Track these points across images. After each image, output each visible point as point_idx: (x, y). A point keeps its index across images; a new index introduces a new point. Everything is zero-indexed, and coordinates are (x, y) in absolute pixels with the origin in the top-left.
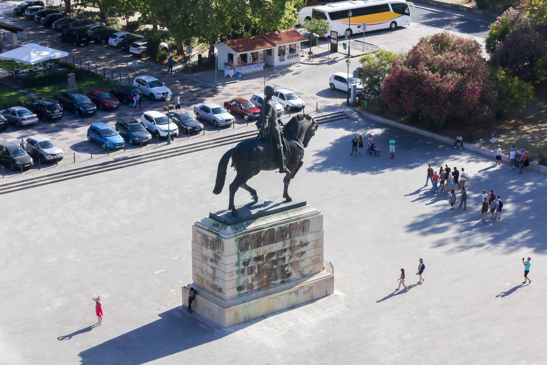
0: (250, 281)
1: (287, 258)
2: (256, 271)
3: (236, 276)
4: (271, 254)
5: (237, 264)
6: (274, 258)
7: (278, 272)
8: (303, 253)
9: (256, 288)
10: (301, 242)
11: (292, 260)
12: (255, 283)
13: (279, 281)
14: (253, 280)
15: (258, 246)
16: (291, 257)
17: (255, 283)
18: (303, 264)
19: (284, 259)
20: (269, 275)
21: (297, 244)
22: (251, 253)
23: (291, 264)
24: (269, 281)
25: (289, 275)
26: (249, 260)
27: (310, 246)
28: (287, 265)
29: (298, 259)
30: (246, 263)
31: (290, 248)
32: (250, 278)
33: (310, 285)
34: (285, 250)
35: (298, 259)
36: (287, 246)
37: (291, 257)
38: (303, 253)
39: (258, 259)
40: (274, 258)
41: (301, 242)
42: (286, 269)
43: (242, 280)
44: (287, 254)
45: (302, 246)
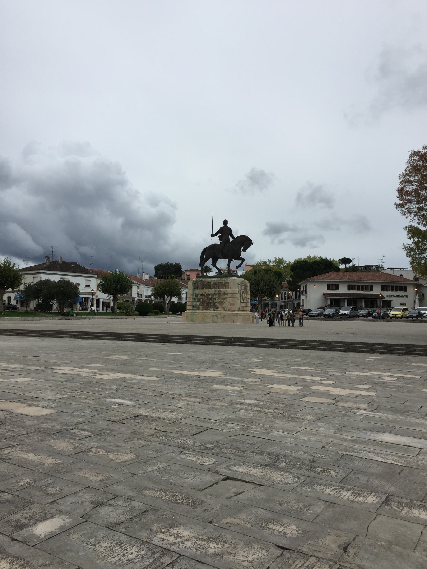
0: (198, 305)
1: (217, 299)
2: (201, 300)
3: (191, 300)
4: (209, 295)
5: (192, 295)
6: (210, 297)
7: (212, 304)
8: (225, 298)
9: (201, 309)
10: (224, 293)
11: (219, 301)
12: (200, 306)
13: (212, 309)
14: (199, 305)
15: (203, 289)
16: (218, 299)
17: (200, 306)
18: (225, 304)
19: (215, 298)
20: (207, 305)
21: (222, 293)
22: (199, 291)
23: (219, 302)
24: (207, 307)
25: (218, 308)
26: (198, 295)
27: (229, 296)
28: (216, 302)
29: (222, 301)
30: (196, 295)
31: (218, 294)
32: (198, 303)
33: (224, 314)
34: (216, 294)
35: (222, 301)
36: (217, 292)
37: (218, 299)
38: (225, 298)
39: (202, 295)
40: (210, 297)
41: (224, 293)
42: (216, 304)
43: (195, 303)
44: (216, 296)
45: (225, 295)
